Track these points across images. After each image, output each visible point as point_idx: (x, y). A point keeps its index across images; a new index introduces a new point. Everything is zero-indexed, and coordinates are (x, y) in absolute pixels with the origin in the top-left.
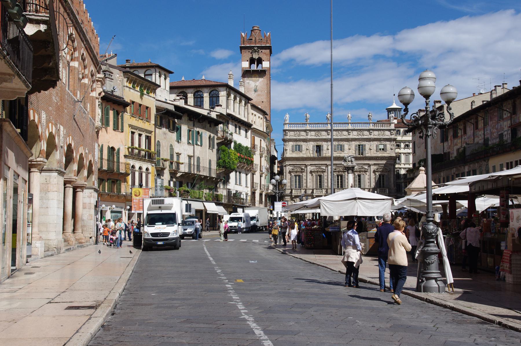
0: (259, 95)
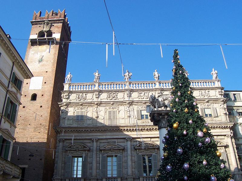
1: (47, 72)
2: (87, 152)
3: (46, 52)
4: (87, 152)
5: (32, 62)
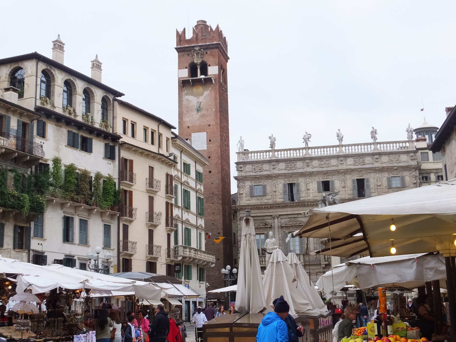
0: (203, 116)
1: (209, 125)
2: (268, 229)
3: (204, 96)
4: (268, 229)
5: (188, 112)
